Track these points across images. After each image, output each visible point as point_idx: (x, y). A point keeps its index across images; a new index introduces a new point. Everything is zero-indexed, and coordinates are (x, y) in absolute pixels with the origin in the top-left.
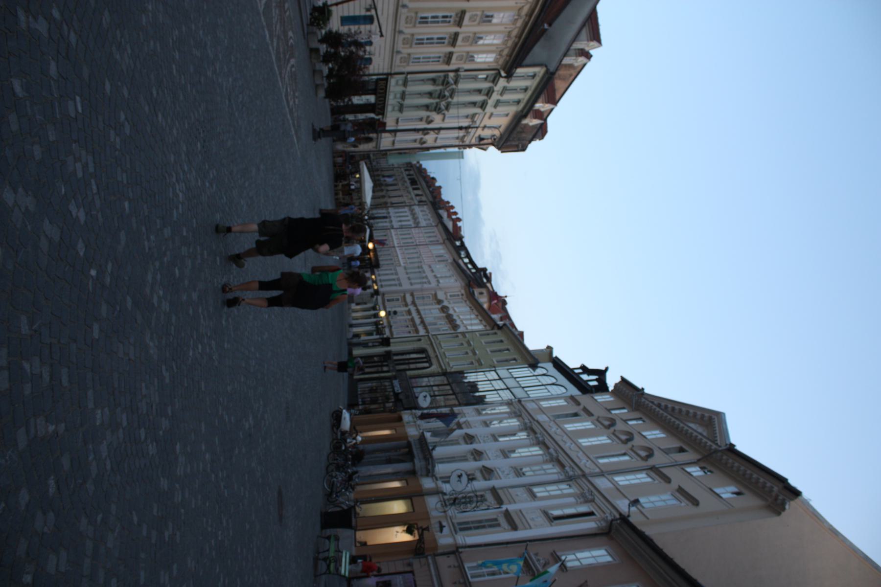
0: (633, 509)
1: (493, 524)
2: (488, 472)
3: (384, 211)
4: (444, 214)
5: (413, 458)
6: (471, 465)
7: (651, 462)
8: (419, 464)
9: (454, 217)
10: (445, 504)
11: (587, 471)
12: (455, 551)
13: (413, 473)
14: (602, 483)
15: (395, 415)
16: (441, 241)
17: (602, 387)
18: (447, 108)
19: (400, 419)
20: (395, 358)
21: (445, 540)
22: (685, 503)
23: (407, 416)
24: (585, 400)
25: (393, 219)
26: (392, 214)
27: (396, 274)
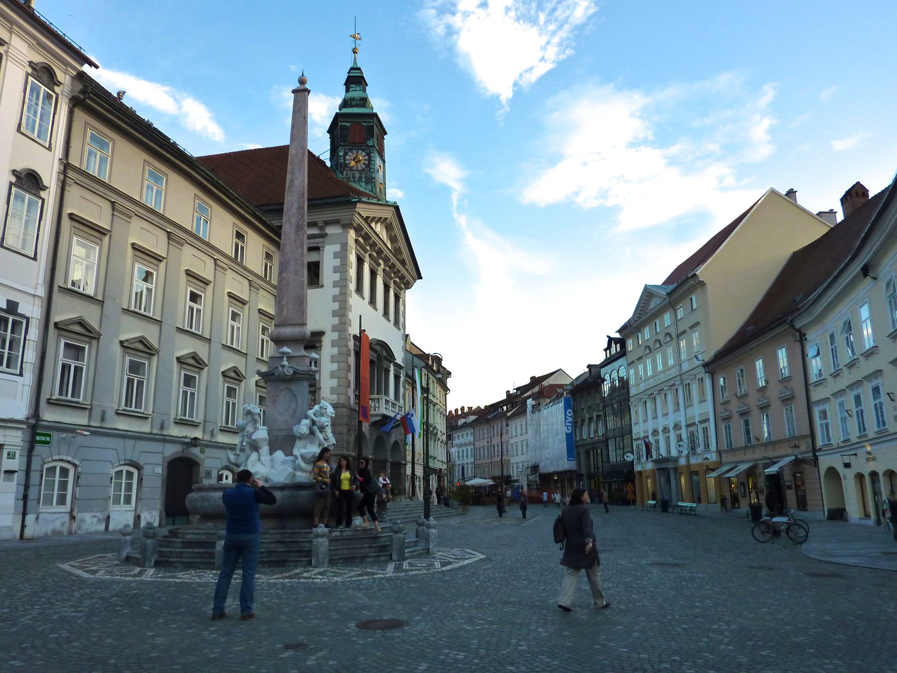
0: (700, 357)
1: (705, 430)
2: (677, 427)
3: (457, 469)
4: (461, 422)
5: (666, 468)
6: (672, 435)
7: (674, 335)
8: (670, 465)
9: (460, 413)
10: (694, 454)
11: (678, 373)
12: (719, 452)
13: (676, 469)
14: (686, 367)
15: (637, 476)
16: (488, 426)
17: (622, 342)
18: (435, 428)
19: (640, 472)
20: (592, 471)
21: (713, 457)
22: (697, 328)
23: (638, 468)
24: (631, 357)
25: (464, 462)
26: (460, 462)
27: (517, 463)
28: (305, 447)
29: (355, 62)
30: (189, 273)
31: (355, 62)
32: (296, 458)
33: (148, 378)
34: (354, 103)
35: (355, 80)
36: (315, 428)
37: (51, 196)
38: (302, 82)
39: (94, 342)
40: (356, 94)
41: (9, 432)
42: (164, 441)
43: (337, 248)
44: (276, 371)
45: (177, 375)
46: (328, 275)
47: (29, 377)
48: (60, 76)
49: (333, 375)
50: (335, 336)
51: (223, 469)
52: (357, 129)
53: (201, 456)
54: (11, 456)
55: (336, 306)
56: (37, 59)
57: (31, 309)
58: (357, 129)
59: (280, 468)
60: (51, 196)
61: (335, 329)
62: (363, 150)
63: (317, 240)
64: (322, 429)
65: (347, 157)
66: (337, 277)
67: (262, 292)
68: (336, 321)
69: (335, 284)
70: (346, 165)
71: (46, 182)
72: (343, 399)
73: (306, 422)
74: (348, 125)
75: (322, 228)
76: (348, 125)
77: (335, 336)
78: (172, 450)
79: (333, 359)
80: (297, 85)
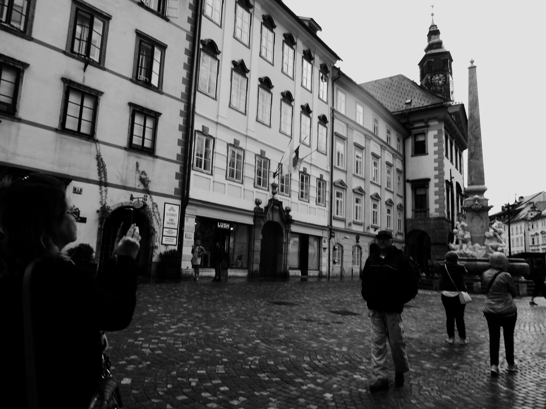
28: (492, 242)
29: (433, 22)
31: (433, 22)
32: (487, 247)
34: (434, 46)
35: (434, 32)
36: (497, 234)
37: (329, 125)
38: (472, 62)
40: (434, 40)
41: (324, 232)
43: (436, 132)
44: (473, 207)
45: (371, 203)
46: (431, 147)
47: (327, 208)
49: (436, 202)
50: (437, 181)
52: (436, 63)
54: (325, 242)
55: (437, 165)
58: (436, 63)
59: (479, 252)
61: (436, 177)
62: (442, 74)
63: (423, 129)
65: (433, 79)
66: (436, 148)
68: (437, 173)
69: (435, 153)
70: (432, 84)
72: (442, 215)
73: (491, 231)
74: (433, 60)
76: (433, 60)
77: (437, 181)
79: (436, 193)
80: (470, 65)
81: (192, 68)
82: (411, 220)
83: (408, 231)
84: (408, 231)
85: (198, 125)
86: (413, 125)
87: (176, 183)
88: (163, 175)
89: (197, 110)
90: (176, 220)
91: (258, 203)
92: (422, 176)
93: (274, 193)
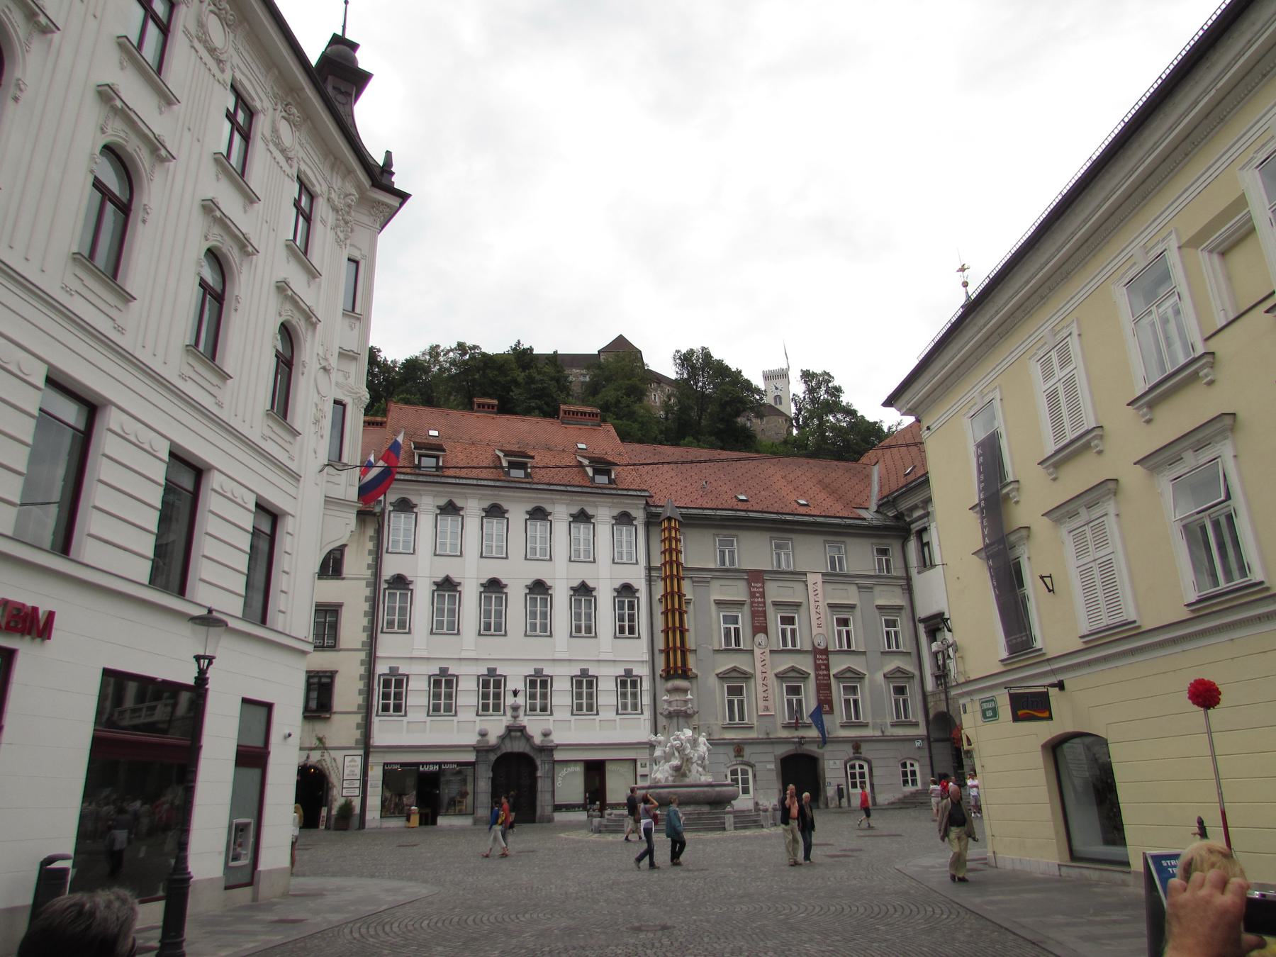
30: (775, 604)
33: (748, 696)
37: (643, 595)
39: (694, 681)
42: (772, 743)
47: (647, 714)
48: (634, 513)
51: (851, 759)
53: (820, 751)
54: (644, 766)
56: (616, 512)
57: (642, 671)
60: (643, 595)
64: (677, 749)
67: (877, 589)
71: (636, 585)
75: (924, 508)
78: (783, 750)
81: (373, 614)
82: (933, 694)
83: (931, 715)
84: (931, 715)
85: (382, 668)
86: (909, 516)
87: (358, 734)
88: (342, 728)
89: (378, 654)
90: (358, 771)
91: (483, 734)
92: (933, 610)
93: (515, 717)
